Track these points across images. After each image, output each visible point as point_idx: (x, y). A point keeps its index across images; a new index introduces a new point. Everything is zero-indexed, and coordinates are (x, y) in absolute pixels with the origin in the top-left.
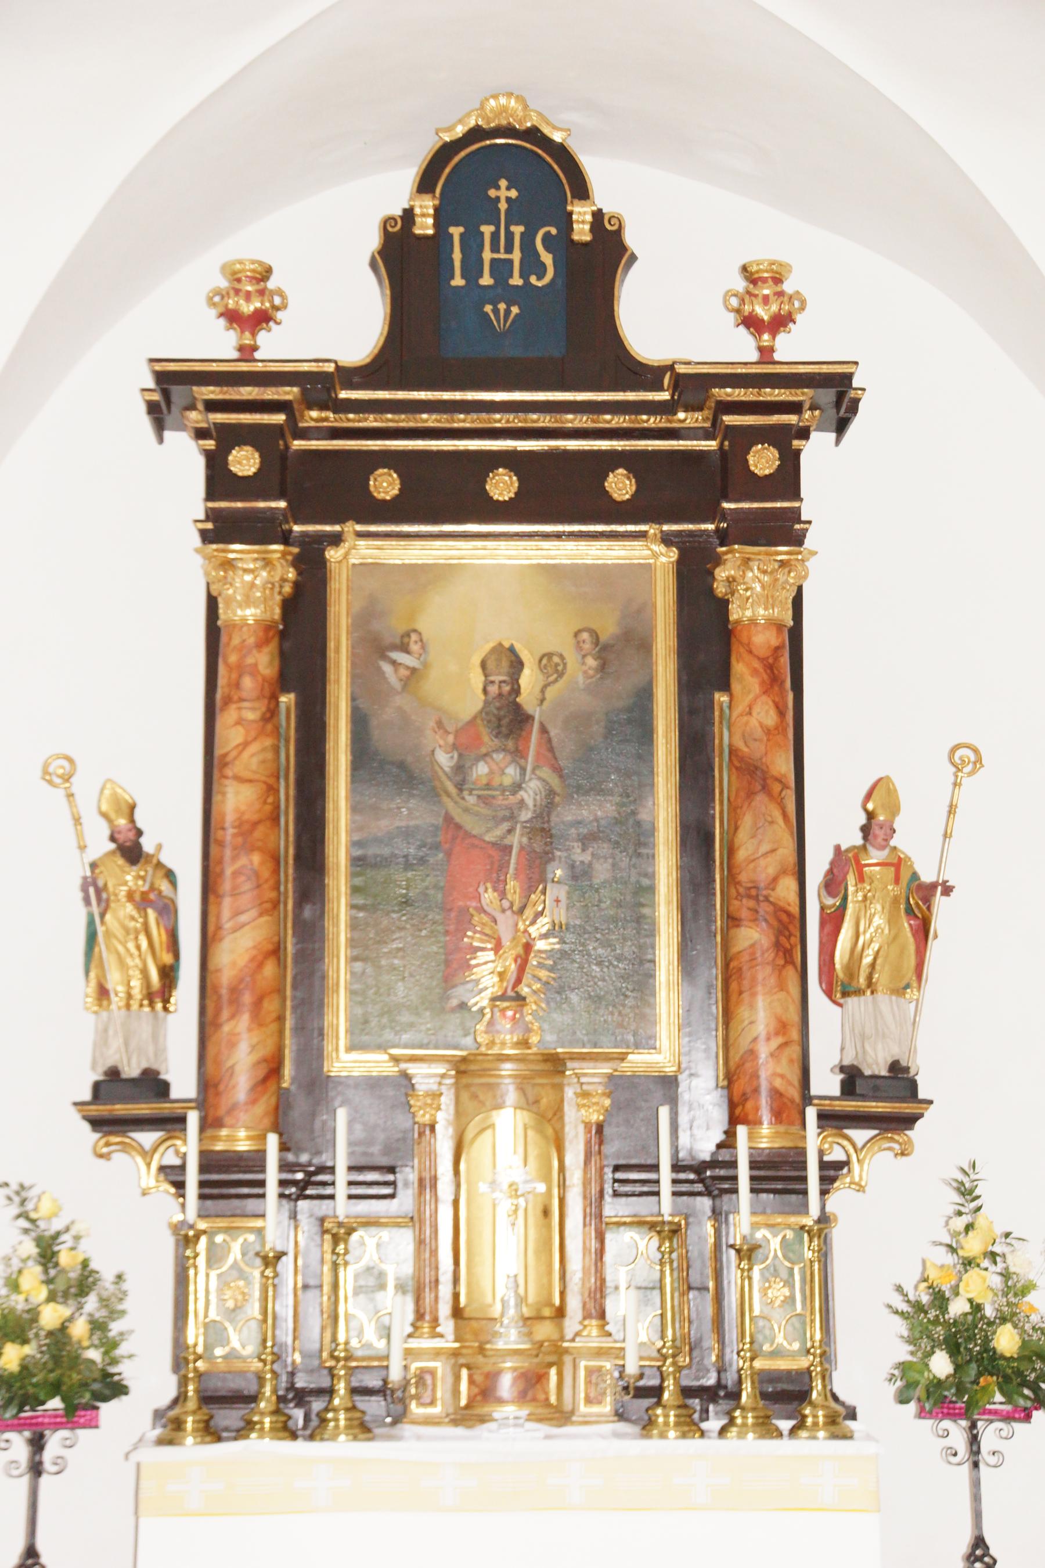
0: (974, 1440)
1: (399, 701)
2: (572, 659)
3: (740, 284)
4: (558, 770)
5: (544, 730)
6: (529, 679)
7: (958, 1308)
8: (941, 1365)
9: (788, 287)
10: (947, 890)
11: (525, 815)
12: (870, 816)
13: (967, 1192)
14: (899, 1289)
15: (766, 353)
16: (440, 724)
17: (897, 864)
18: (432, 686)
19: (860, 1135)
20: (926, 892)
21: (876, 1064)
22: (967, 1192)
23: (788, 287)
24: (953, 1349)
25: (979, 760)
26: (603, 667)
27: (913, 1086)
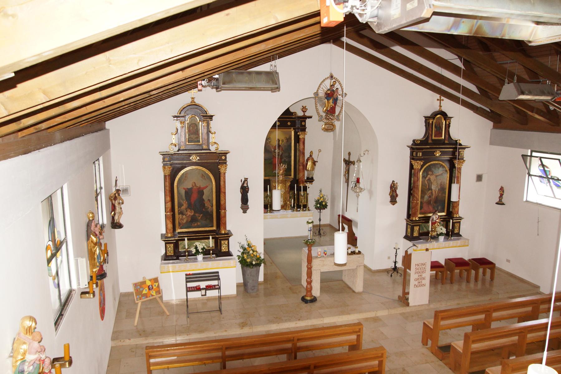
0: (320, 211)
1: (269, 144)
2: (284, 140)
3: (302, 108)
4: (283, 151)
5: (282, 147)
6: (280, 142)
7: (320, 201)
8: (318, 205)
9: (306, 108)
10: (317, 162)
11: (280, 155)
12: (310, 155)
13: (321, 191)
14: (315, 199)
15: (304, 114)
16: (272, 147)
17: (313, 159)
18: (272, 143)
19: (308, 183)
20: (315, 162)
21: (310, 177)
22: (321, 191)
23: (306, 108)
24: (319, 204)
25: (321, 151)
26: (287, 141)
27: (313, 179)
